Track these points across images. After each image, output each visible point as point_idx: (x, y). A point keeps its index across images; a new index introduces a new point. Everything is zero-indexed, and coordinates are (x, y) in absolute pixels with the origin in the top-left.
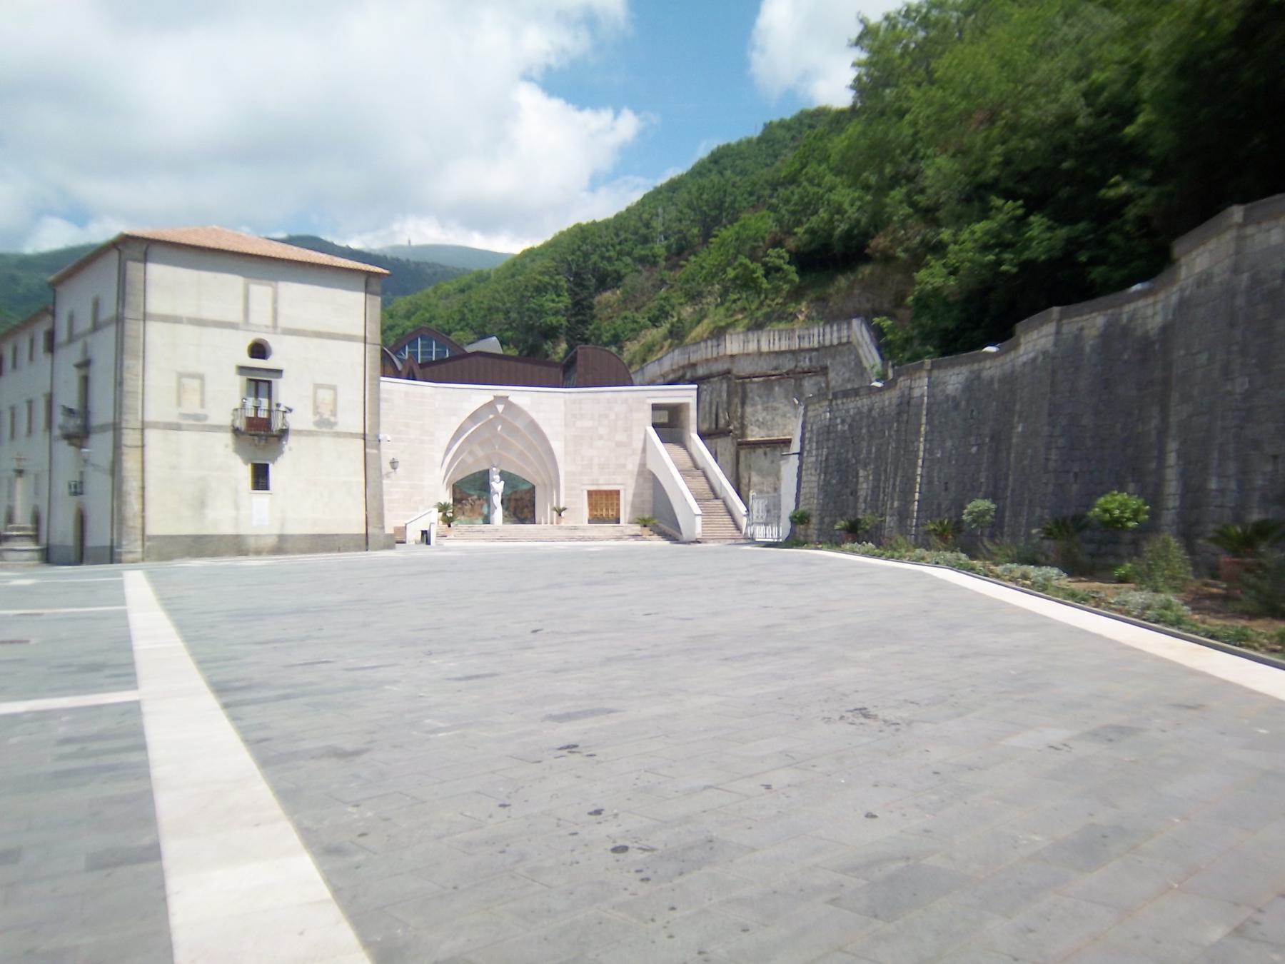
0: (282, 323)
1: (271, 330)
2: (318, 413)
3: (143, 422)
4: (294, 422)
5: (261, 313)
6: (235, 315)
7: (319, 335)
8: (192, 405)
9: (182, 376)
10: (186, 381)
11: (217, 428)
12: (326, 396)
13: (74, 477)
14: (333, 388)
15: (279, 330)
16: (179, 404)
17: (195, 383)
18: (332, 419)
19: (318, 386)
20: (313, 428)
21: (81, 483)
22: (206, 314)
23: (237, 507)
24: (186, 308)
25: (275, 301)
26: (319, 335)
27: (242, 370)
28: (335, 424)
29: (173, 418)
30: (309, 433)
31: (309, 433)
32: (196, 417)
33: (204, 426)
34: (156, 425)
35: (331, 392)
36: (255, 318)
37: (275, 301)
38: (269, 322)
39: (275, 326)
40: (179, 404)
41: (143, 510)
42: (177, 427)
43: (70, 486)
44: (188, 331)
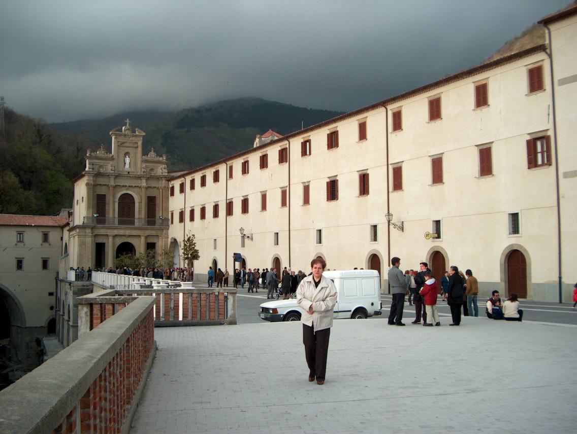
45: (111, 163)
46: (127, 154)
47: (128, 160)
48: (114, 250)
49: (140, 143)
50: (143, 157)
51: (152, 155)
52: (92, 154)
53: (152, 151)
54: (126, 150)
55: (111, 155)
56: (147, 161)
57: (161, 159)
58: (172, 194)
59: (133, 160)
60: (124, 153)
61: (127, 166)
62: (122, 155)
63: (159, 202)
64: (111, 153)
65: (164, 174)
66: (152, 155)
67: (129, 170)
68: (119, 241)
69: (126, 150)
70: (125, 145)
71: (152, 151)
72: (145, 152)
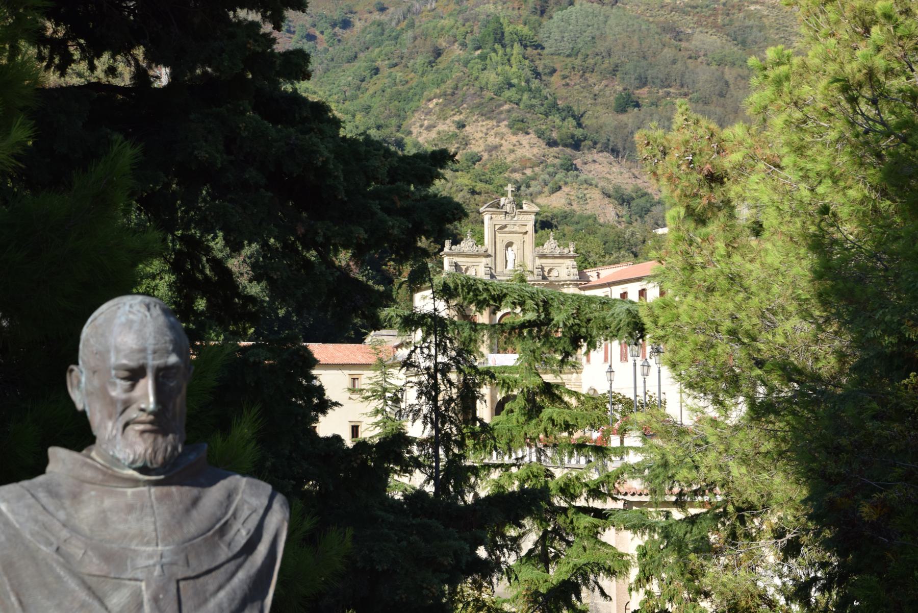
45: (484, 261)
46: (510, 244)
49: (530, 227)
50: (537, 248)
52: (453, 247)
53: (551, 238)
54: (509, 238)
55: (484, 248)
57: (566, 251)
59: (521, 252)
60: (505, 243)
62: (500, 246)
64: (482, 244)
65: (572, 277)
69: (509, 238)
70: (506, 230)
71: (551, 238)
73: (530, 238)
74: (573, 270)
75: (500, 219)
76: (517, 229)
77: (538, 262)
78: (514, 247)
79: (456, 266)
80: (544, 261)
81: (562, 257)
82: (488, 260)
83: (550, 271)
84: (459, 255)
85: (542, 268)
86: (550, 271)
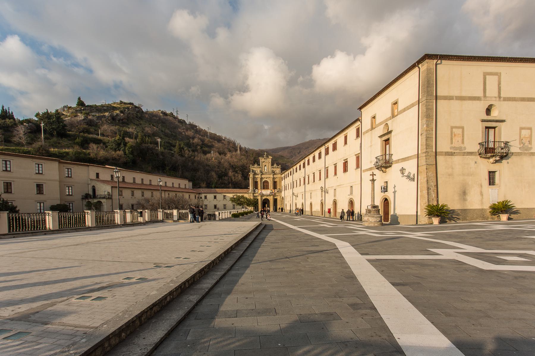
0: (502, 95)
1: (498, 99)
2: (522, 143)
3: (436, 152)
4: (513, 150)
5: (492, 91)
6: (480, 94)
7: (523, 99)
8: (457, 143)
9: (452, 128)
10: (454, 130)
11: (471, 153)
12: (525, 133)
13: (383, 184)
14: (530, 129)
15: (502, 99)
16: (452, 143)
17: (460, 131)
18: (530, 146)
19: (521, 129)
20: (519, 151)
21: (387, 187)
22: (464, 94)
23: (482, 194)
24: (456, 93)
25: (499, 84)
26: (523, 99)
27: (483, 121)
28: (531, 148)
29: (450, 150)
30: (518, 154)
31: (518, 154)
32: (460, 148)
33: (464, 153)
34: (442, 153)
35: (529, 131)
36: (488, 94)
37: (499, 84)
38: (497, 96)
39: (500, 97)
40: (452, 143)
41: (438, 197)
42: (451, 154)
43: (382, 188)
44: (455, 103)
46: (265, 165)
47: (266, 168)
48: (261, 201)
49: (270, 162)
51: (275, 165)
56: (273, 168)
57: (279, 167)
58: (282, 180)
61: (266, 170)
63: (278, 183)
64: (259, 165)
66: (275, 165)
67: (267, 171)
68: (264, 198)
69: (265, 164)
72: (272, 165)
73: (270, 164)
74: (280, 171)
75: (263, 160)
76: (267, 162)
77: (272, 169)
78: (267, 166)
79: (253, 170)
80: (273, 169)
81: (277, 168)
82: (260, 169)
83: (275, 171)
84: (254, 168)
85: (273, 170)
86: (275, 171)
